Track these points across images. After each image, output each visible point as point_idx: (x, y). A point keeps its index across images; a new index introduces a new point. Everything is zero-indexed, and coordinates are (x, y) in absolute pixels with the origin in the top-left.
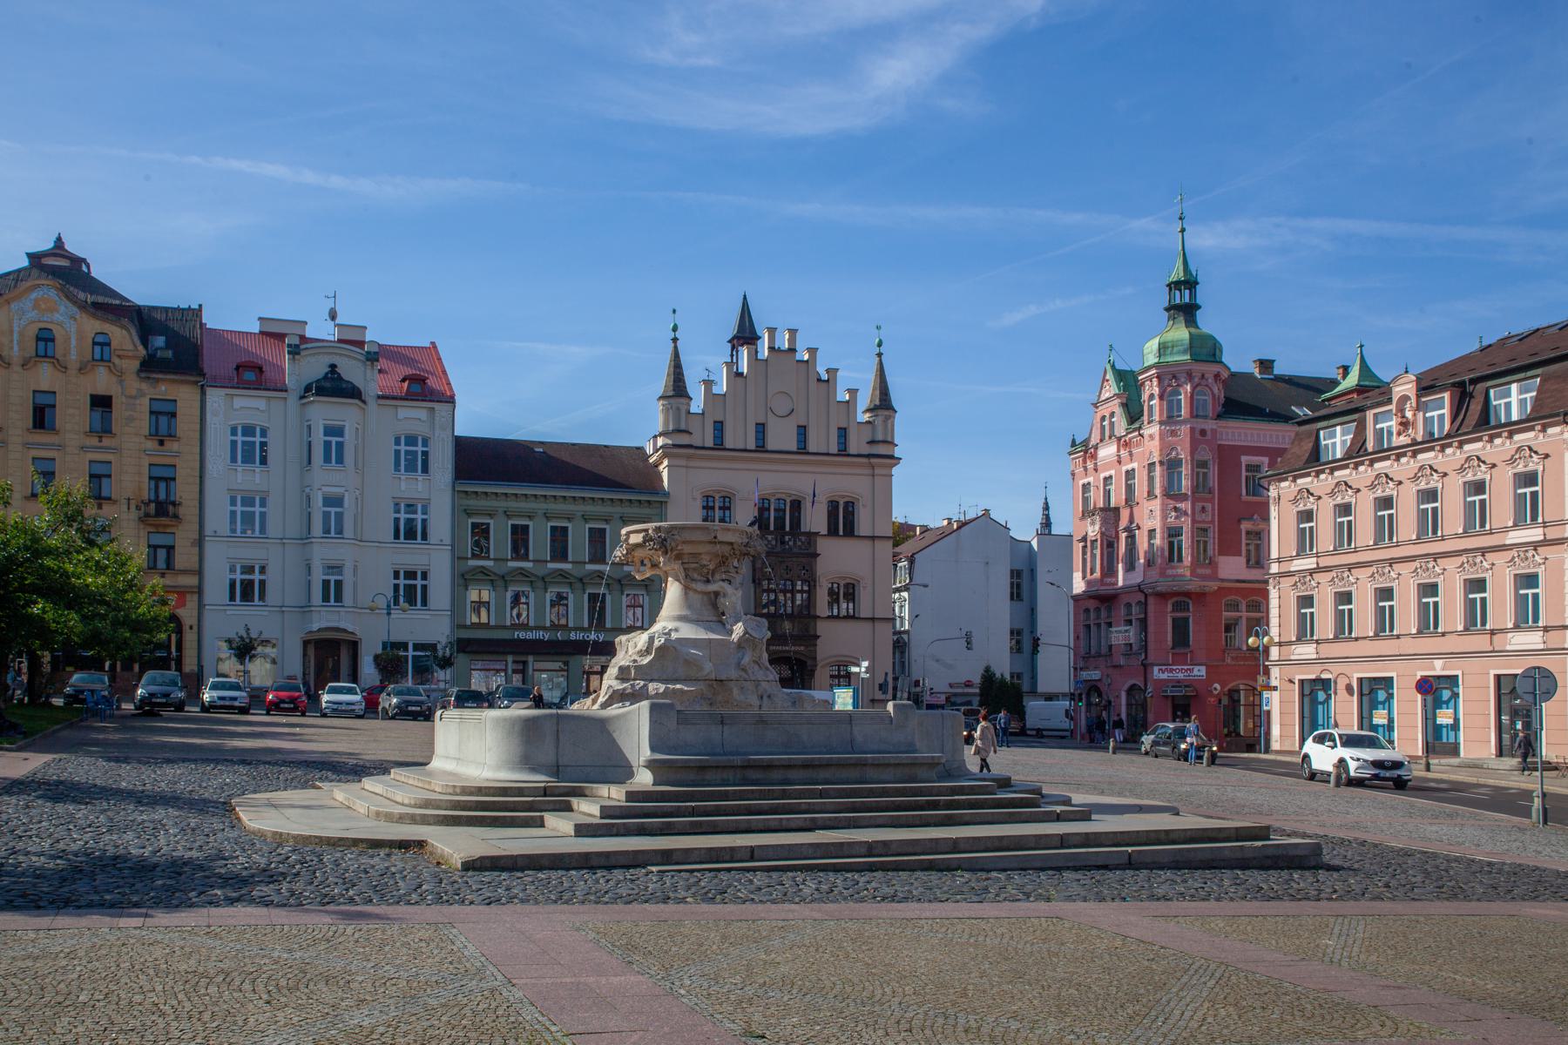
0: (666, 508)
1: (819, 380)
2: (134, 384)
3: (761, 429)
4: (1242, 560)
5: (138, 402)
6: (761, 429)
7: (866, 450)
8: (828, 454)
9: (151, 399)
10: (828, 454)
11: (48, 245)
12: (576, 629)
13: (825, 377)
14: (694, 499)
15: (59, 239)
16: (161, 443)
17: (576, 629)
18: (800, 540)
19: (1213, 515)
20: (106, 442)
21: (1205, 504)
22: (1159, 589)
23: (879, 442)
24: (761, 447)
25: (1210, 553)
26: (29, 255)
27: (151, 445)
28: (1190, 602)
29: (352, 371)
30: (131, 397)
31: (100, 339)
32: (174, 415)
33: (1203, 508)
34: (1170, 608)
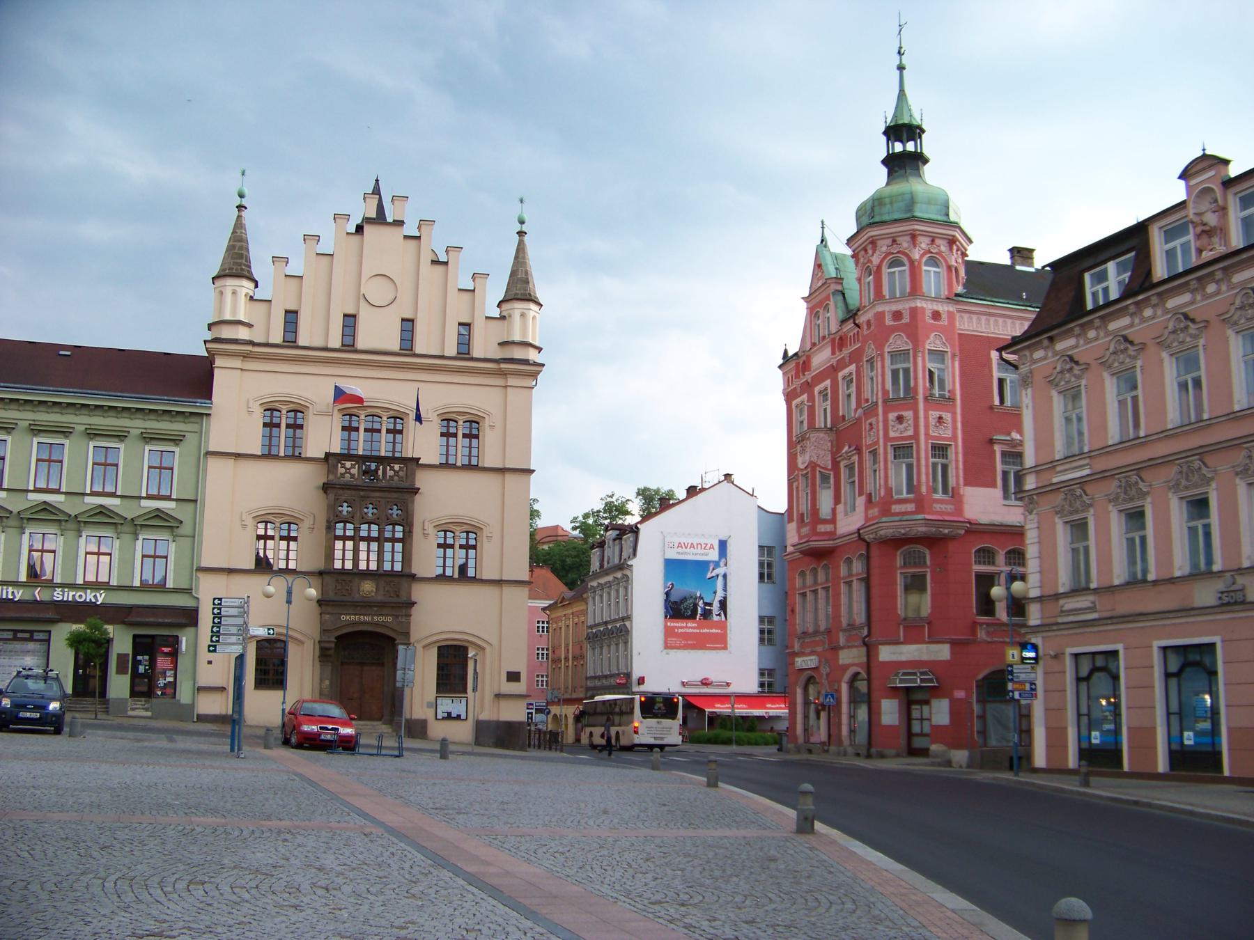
0: (209, 425)
1: (435, 262)
3: (350, 321)
4: (998, 492)
6: (350, 321)
7: (497, 353)
8: (442, 357)
10: (442, 357)
12: (63, 586)
13: (443, 258)
14: (250, 413)
17: (63, 586)
18: (392, 469)
19: (954, 429)
21: (944, 415)
22: (882, 532)
23: (513, 343)
24: (349, 345)
25: (952, 482)
28: (927, 552)
33: (940, 418)
34: (899, 561)
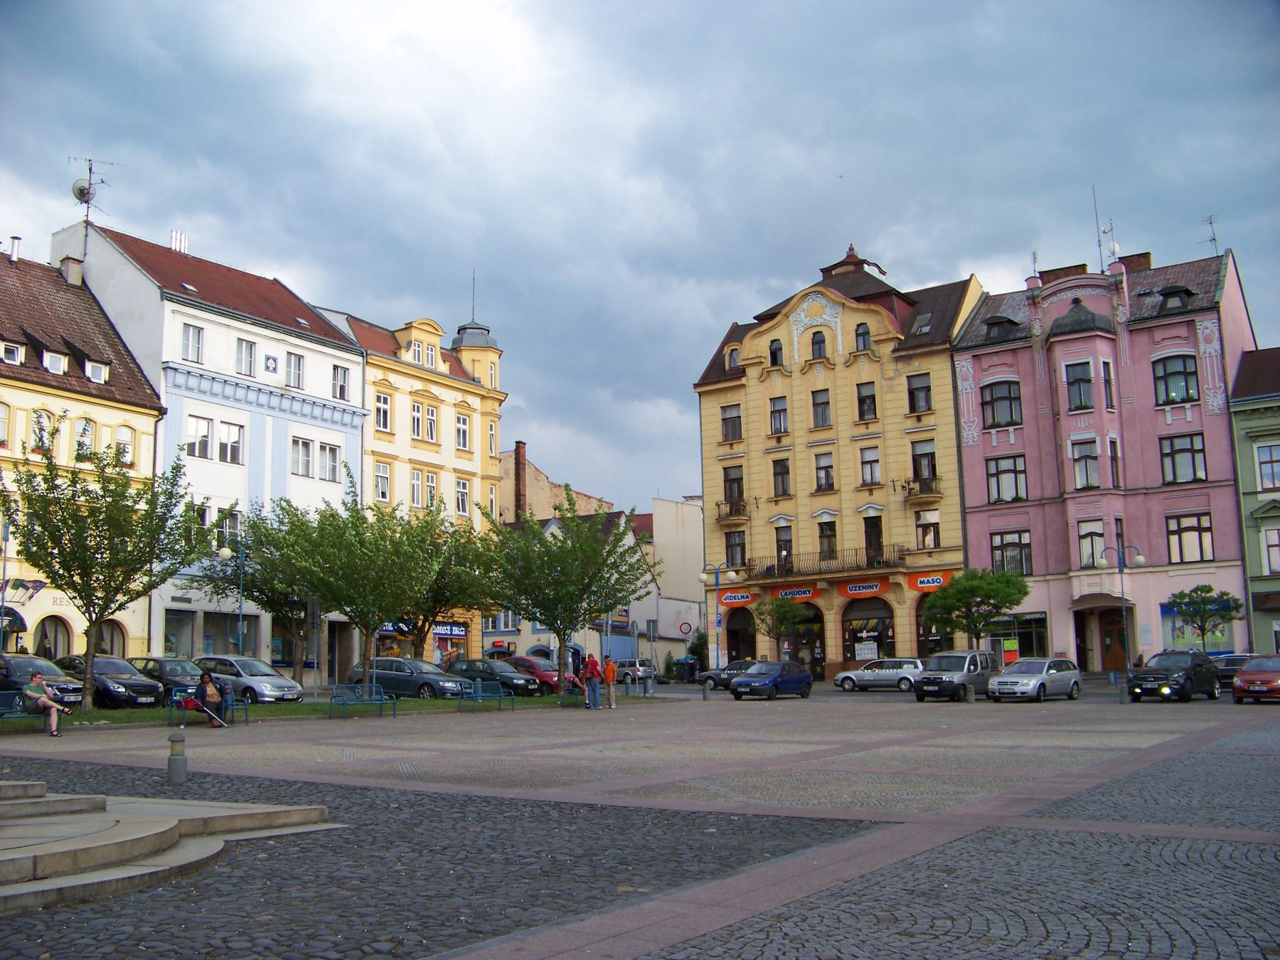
2: (891, 368)
5: (896, 382)
9: (908, 377)
11: (842, 256)
15: (851, 249)
16: (919, 419)
20: (872, 428)
26: (822, 270)
27: (911, 423)
29: (1095, 303)
30: (890, 379)
31: (861, 331)
32: (928, 389)
